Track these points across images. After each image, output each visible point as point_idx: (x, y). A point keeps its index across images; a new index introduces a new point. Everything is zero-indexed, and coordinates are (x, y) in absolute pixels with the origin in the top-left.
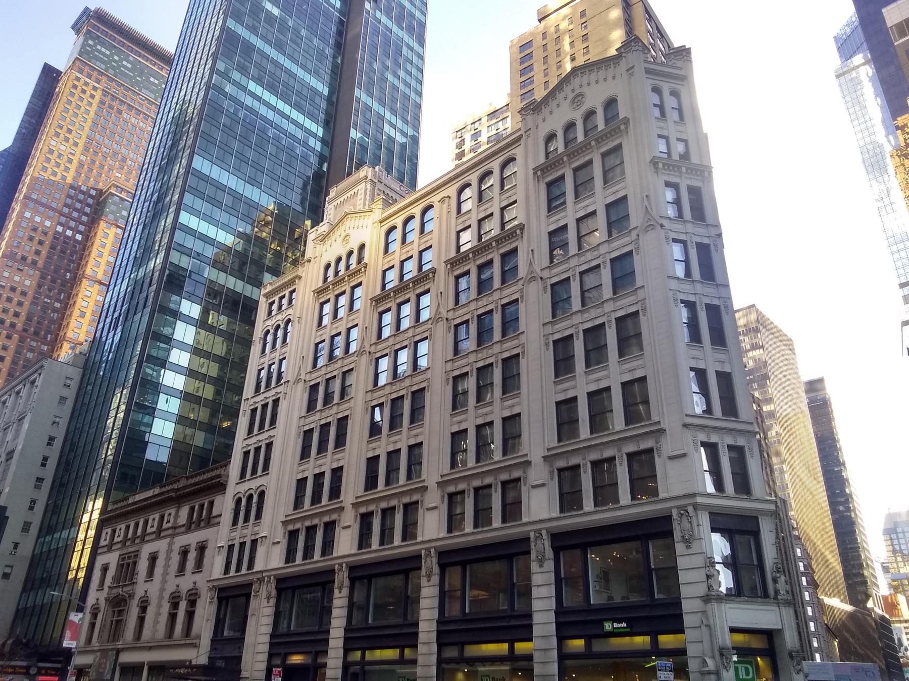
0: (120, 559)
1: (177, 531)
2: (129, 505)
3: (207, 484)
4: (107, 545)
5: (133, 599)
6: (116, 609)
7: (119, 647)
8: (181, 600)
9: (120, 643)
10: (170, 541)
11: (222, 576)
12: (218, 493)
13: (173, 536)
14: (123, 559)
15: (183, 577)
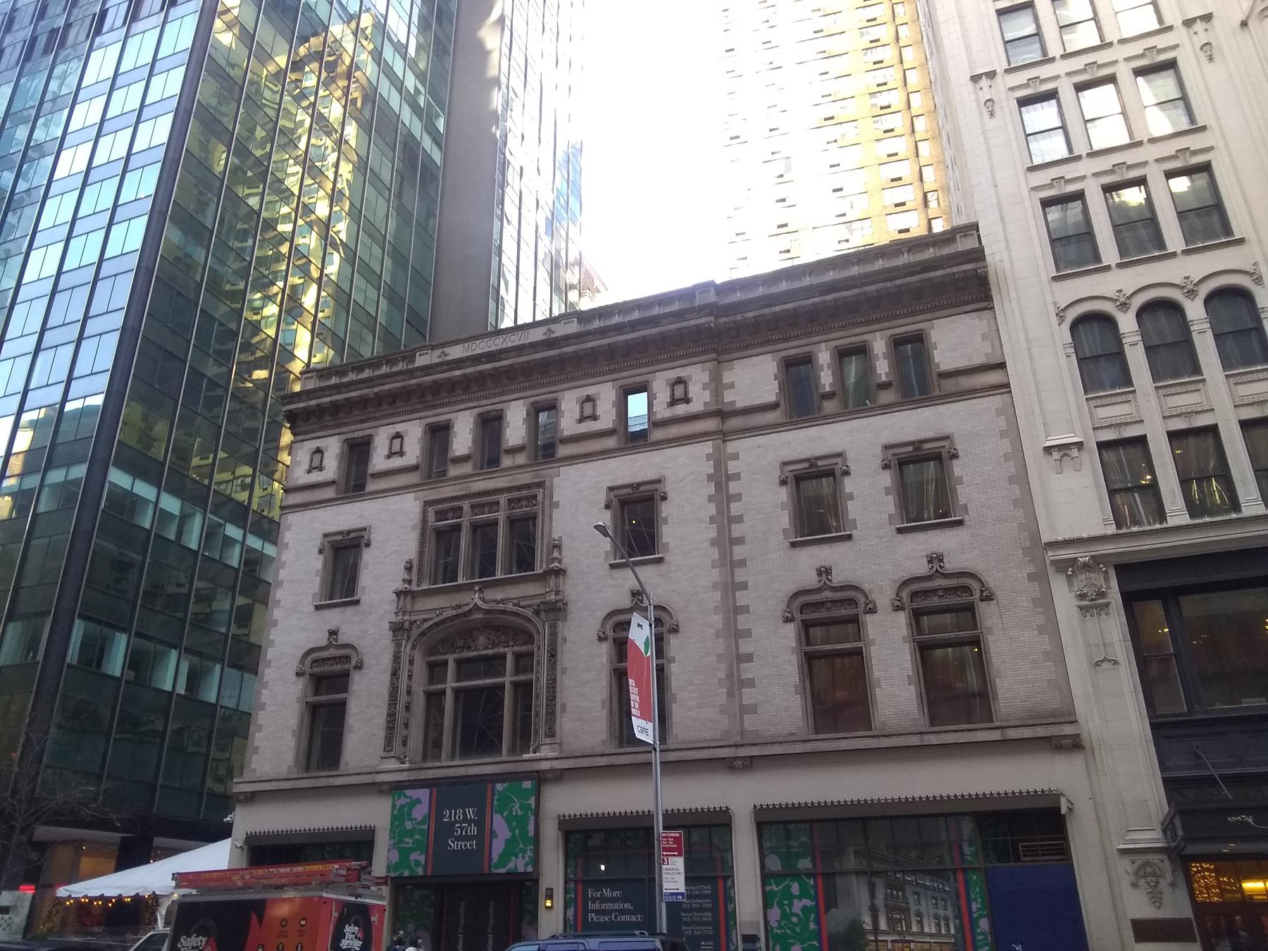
0: (431, 517)
1: (734, 423)
2: (411, 373)
3: (898, 282)
4: (333, 482)
5: (565, 620)
6: (451, 659)
7: (545, 766)
8: (873, 611)
9: (545, 752)
10: (717, 450)
11: (1112, 530)
12: (938, 314)
13: (724, 436)
14: (441, 515)
15: (847, 544)
